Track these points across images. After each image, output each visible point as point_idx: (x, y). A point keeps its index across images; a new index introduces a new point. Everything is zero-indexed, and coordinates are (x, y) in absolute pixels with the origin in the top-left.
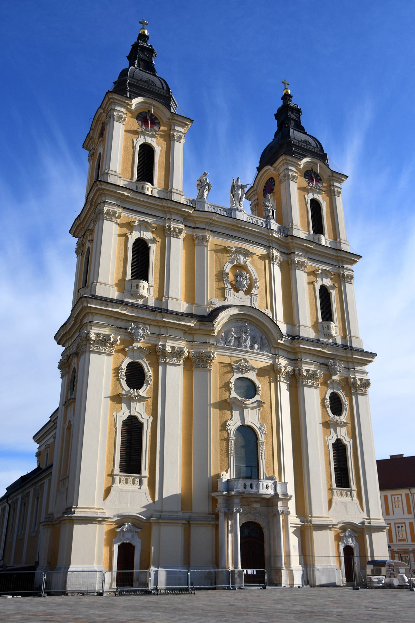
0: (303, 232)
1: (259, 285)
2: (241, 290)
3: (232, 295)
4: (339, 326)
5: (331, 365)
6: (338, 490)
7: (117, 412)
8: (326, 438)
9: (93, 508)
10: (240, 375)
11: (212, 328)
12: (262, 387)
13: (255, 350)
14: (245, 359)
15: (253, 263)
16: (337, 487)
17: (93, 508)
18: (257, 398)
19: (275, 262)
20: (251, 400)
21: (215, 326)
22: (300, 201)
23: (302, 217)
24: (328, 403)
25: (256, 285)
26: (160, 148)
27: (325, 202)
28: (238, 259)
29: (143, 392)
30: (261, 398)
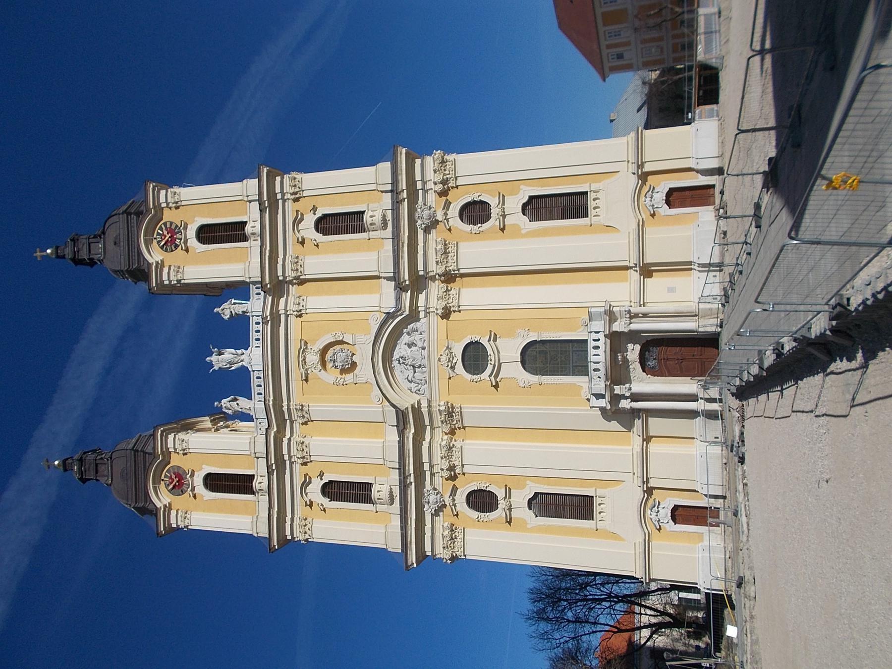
0: (249, 260)
1: (340, 333)
2: (352, 359)
3: (360, 374)
4: (367, 203)
5: (424, 224)
6: (591, 215)
7: (527, 524)
8: (523, 232)
9: (635, 554)
10: (460, 363)
11: (410, 409)
12: (471, 334)
13: (425, 344)
14: (439, 360)
15: (314, 341)
16: (588, 217)
17: (635, 554)
18: (484, 341)
19: (303, 306)
20: (490, 351)
21: (407, 406)
22: (208, 262)
23: (229, 260)
24: (475, 227)
25: (341, 338)
26: (204, 466)
27: (196, 219)
28: (313, 363)
29: (500, 493)
30: (484, 337)
